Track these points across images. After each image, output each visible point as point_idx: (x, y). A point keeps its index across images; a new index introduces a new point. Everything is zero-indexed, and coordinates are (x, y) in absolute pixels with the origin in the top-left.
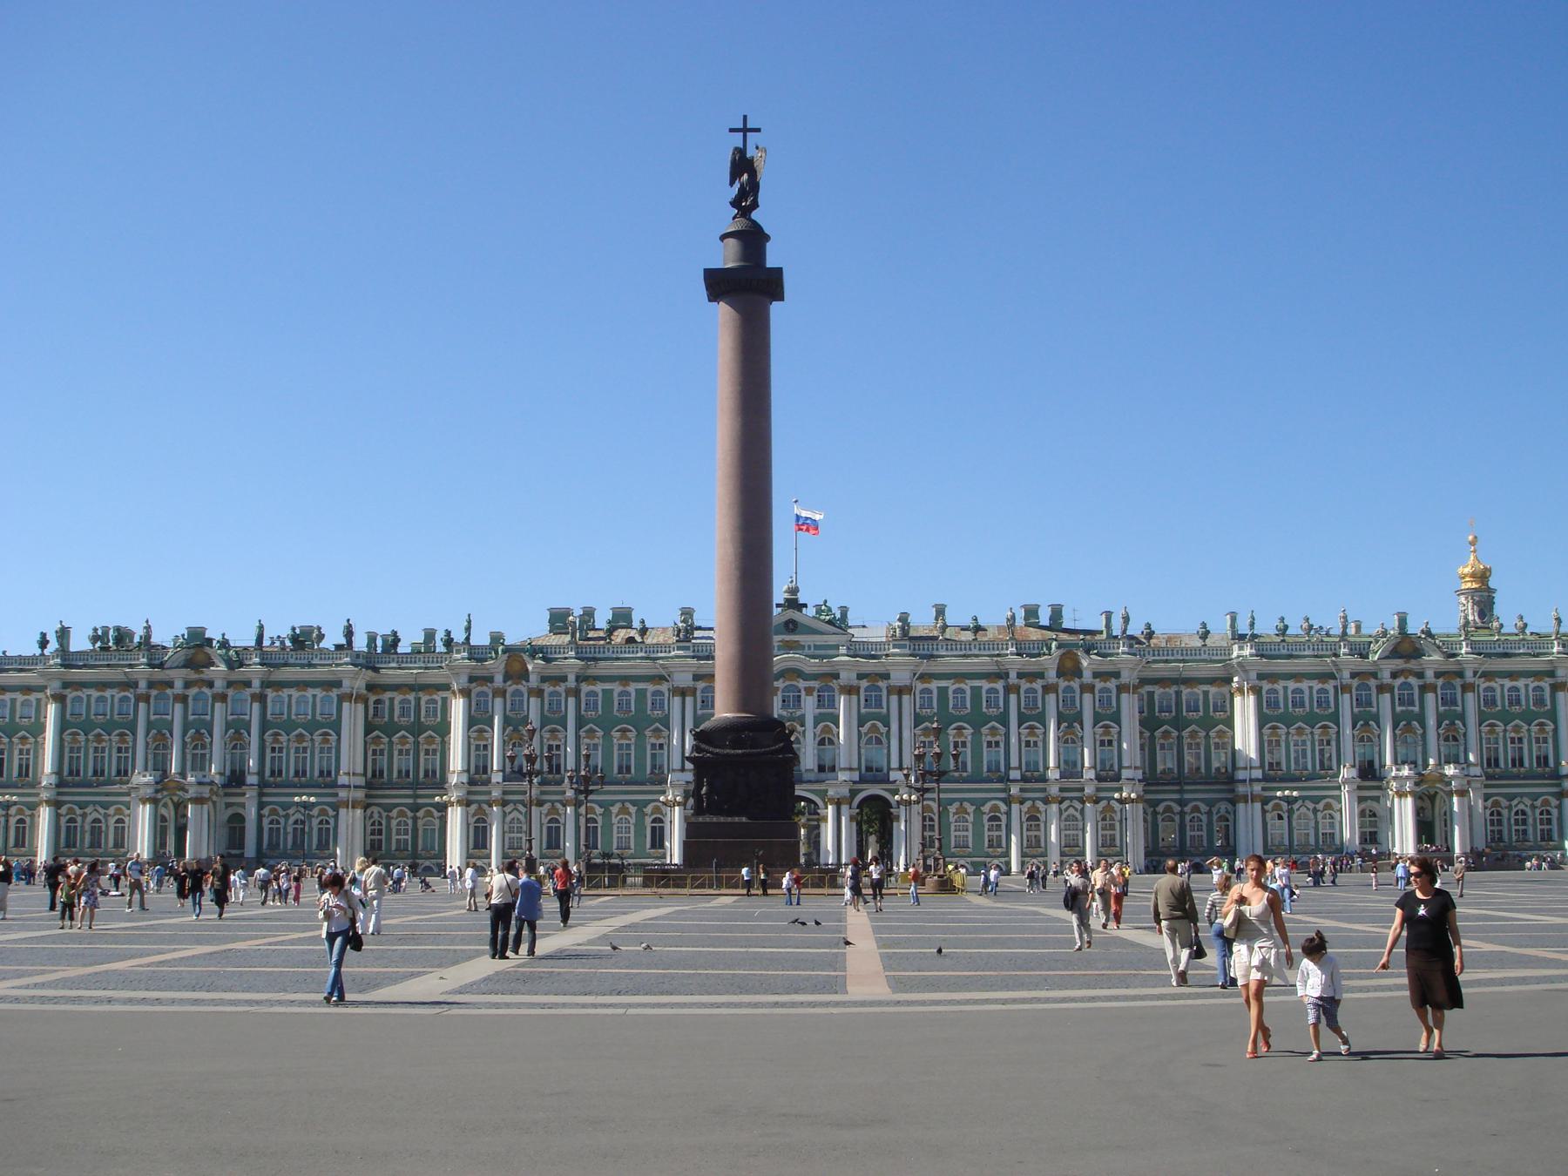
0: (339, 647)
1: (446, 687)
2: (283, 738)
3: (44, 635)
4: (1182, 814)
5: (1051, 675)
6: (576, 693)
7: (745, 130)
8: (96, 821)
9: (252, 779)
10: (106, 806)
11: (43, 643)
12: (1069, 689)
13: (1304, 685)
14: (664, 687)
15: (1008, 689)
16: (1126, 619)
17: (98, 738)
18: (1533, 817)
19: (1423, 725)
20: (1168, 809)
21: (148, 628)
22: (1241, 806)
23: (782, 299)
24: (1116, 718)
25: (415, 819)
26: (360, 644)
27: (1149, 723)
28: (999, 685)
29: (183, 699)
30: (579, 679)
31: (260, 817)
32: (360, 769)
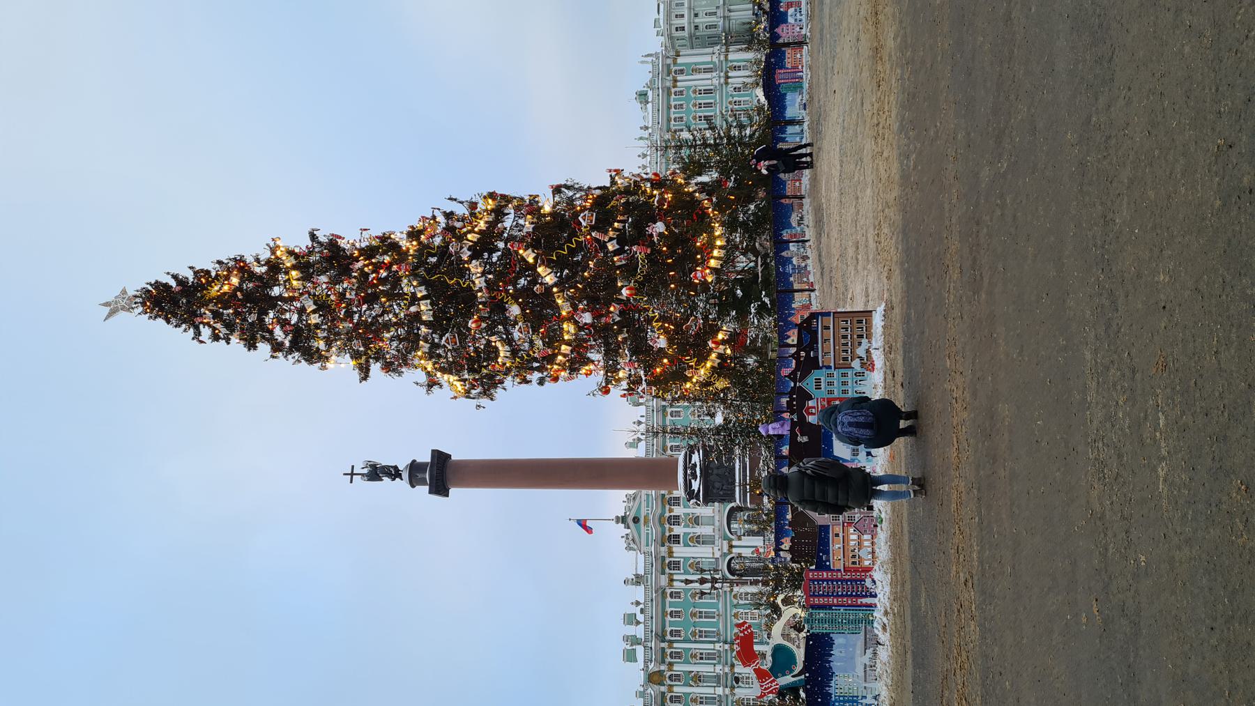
6: (671, 642)
14: (668, 591)
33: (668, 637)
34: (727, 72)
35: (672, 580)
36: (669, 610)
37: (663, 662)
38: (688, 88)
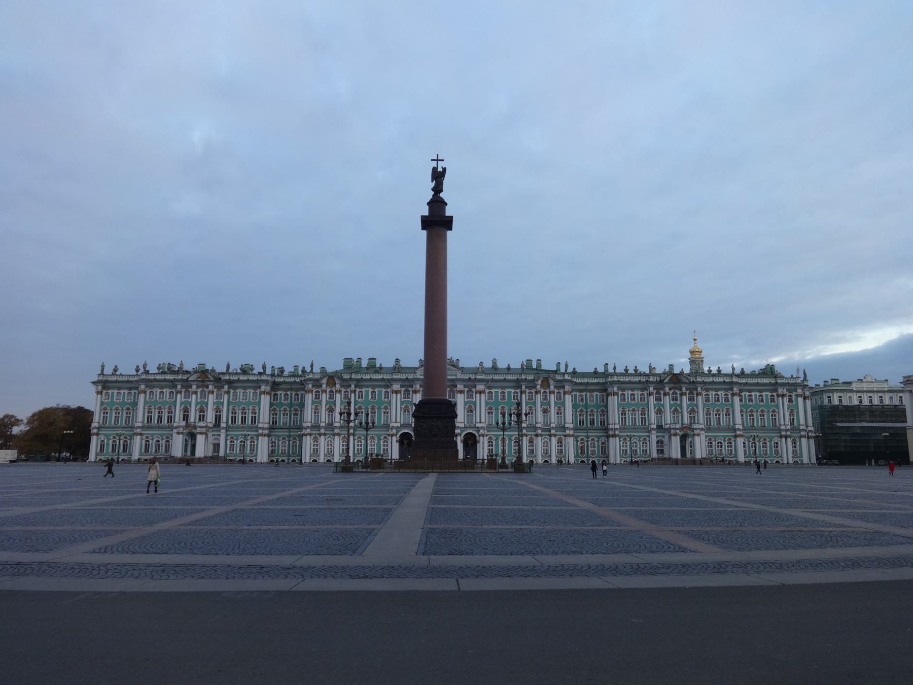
0: (260, 374)
1: (303, 389)
2: (237, 408)
3: (138, 367)
4: (587, 441)
5: (539, 387)
6: (355, 392)
7: (437, 160)
8: (158, 441)
9: (223, 425)
10: (162, 435)
11: (137, 370)
12: (545, 392)
13: (635, 392)
14: (389, 390)
15: (522, 393)
16: (567, 366)
17: (160, 408)
18: (725, 444)
19: (681, 409)
20: (582, 439)
21: (182, 364)
22: (611, 439)
23: (451, 229)
24: (564, 404)
25: (289, 441)
26: (269, 371)
27: (575, 406)
28: (518, 391)
29: (196, 393)
30: (356, 387)
31: (226, 440)
32: (267, 421)
33: (358, 390)
34: (790, 437)
35: (396, 392)
36: (377, 390)
37: (342, 386)
38: (777, 406)
